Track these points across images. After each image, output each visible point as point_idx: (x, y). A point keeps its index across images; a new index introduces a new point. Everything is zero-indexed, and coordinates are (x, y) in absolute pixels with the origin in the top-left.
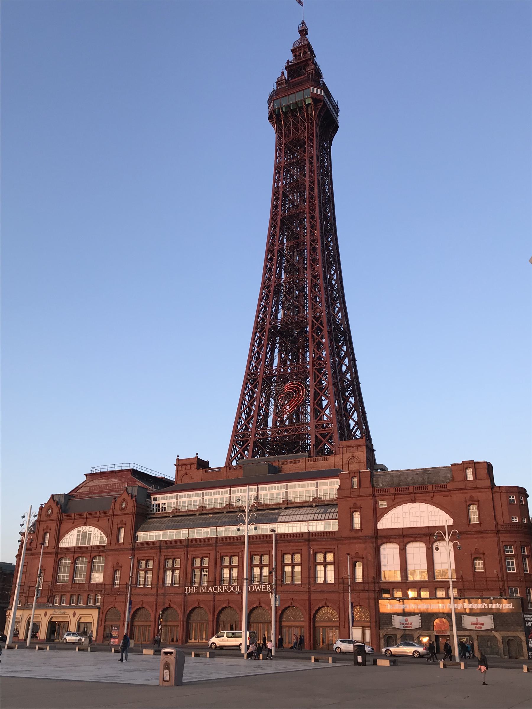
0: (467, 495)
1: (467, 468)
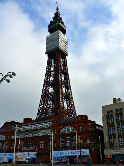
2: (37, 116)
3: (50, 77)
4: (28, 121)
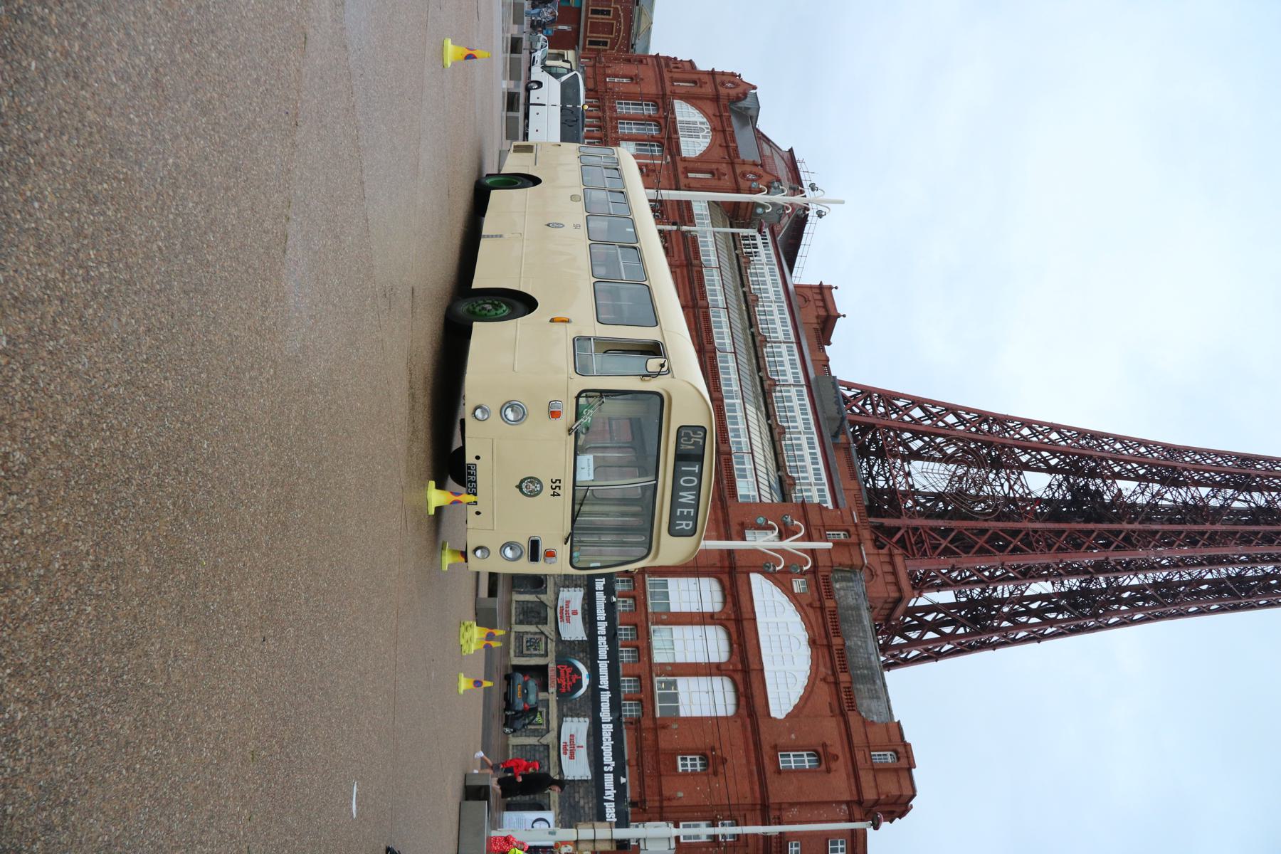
0: (837, 748)
1: (896, 752)
2: (850, 386)
3: (1051, 470)
4: (817, 314)
